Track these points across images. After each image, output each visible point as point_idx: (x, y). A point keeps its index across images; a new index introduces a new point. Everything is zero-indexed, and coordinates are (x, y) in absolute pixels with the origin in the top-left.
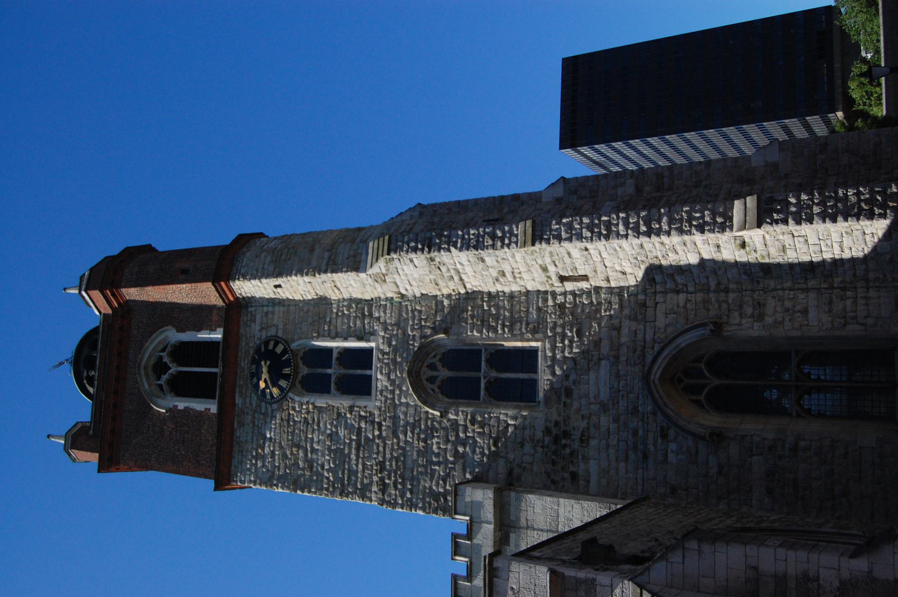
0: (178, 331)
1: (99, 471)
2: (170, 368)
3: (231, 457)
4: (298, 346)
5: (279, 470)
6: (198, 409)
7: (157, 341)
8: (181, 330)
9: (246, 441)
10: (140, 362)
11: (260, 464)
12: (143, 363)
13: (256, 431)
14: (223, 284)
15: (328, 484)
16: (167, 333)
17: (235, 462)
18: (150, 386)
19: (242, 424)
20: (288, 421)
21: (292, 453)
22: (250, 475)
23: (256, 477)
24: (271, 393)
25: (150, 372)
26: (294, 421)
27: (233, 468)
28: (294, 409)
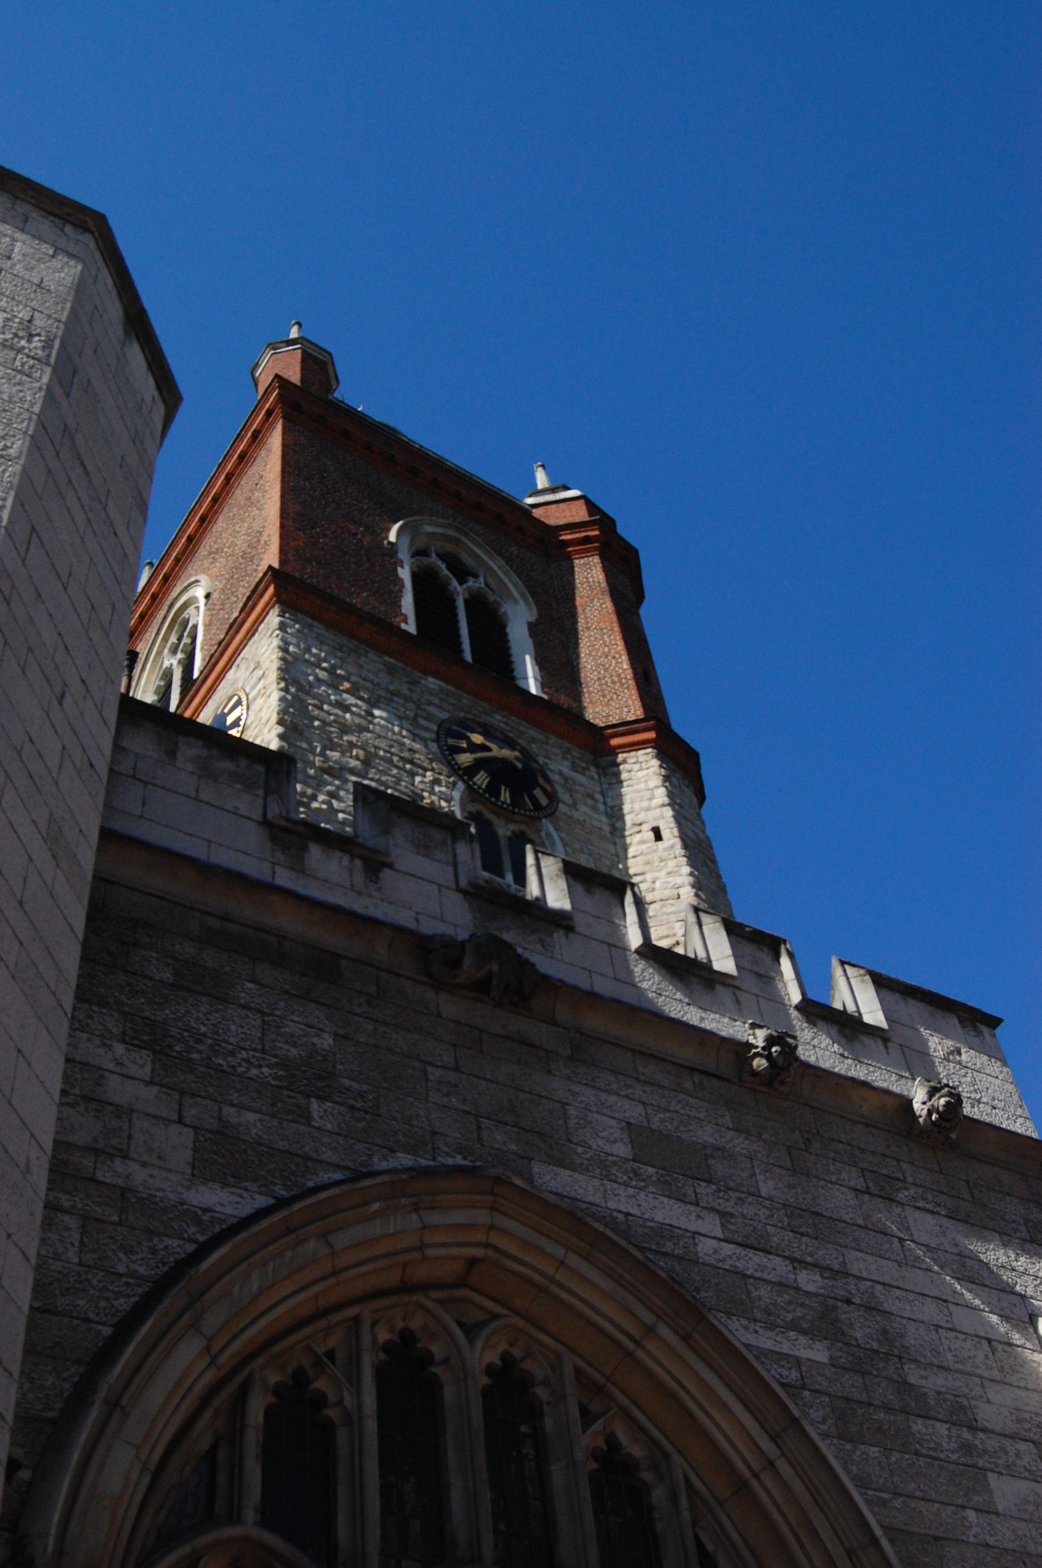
0: (531, 626)
1: (277, 376)
2: (461, 584)
3: (330, 625)
4: (549, 835)
5: (314, 705)
6: (403, 602)
7: (506, 580)
8: (533, 629)
9: (360, 667)
10: (466, 535)
11: (323, 675)
12: (464, 539)
13: (382, 693)
14: (652, 735)
15: (303, 794)
16: (521, 602)
17: (320, 628)
18: (428, 534)
19: (391, 671)
20: (411, 762)
21: (352, 745)
22: (298, 646)
23: (296, 658)
24: (463, 751)
25: (449, 547)
26: (412, 775)
27: (308, 620)
28: (436, 782)
